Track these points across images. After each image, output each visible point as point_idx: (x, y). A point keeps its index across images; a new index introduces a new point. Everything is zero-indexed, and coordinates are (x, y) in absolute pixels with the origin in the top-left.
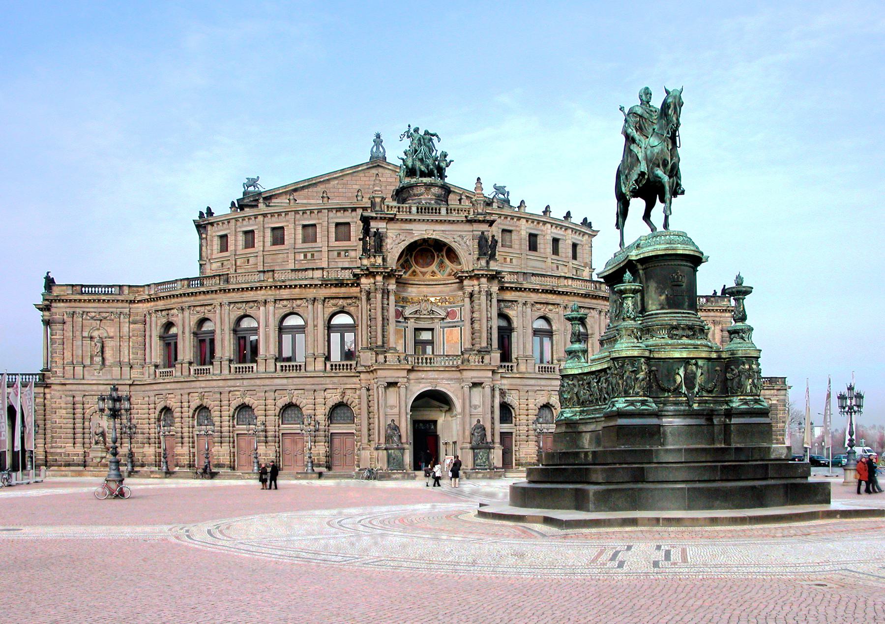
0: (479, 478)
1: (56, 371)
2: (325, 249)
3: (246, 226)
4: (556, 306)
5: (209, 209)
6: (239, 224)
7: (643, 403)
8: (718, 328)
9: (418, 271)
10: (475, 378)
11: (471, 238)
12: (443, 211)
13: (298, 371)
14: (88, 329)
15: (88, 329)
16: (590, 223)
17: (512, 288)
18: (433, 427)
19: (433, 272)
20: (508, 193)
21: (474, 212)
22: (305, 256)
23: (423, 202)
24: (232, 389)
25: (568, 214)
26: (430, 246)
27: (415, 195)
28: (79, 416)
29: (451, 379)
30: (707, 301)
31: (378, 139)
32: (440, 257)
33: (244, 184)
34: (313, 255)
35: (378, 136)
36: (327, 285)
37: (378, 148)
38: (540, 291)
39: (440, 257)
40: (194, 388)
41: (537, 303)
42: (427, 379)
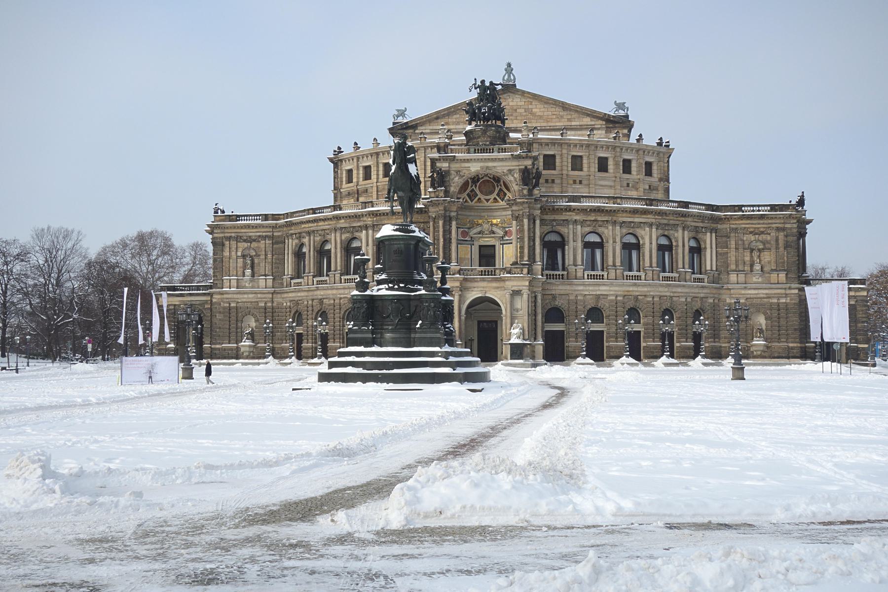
1: (217, 284)
3: (365, 162)
5: (339, 148)
6: (361, 160)
8: (782, 234)
9: (482, 199)
14: (240, 250)
15: (240, 250)
18: (494, 326)
19: (495, 199)
23: (481, 143)
24: (342, 296)
26: (490, 178)
27: (475, 138)
28: (233, 318)
29: (498, 288)
35: (509, 65)
37: (509, 76)
40: (316, 295)
41: (586, 220)
42: (478, 287)
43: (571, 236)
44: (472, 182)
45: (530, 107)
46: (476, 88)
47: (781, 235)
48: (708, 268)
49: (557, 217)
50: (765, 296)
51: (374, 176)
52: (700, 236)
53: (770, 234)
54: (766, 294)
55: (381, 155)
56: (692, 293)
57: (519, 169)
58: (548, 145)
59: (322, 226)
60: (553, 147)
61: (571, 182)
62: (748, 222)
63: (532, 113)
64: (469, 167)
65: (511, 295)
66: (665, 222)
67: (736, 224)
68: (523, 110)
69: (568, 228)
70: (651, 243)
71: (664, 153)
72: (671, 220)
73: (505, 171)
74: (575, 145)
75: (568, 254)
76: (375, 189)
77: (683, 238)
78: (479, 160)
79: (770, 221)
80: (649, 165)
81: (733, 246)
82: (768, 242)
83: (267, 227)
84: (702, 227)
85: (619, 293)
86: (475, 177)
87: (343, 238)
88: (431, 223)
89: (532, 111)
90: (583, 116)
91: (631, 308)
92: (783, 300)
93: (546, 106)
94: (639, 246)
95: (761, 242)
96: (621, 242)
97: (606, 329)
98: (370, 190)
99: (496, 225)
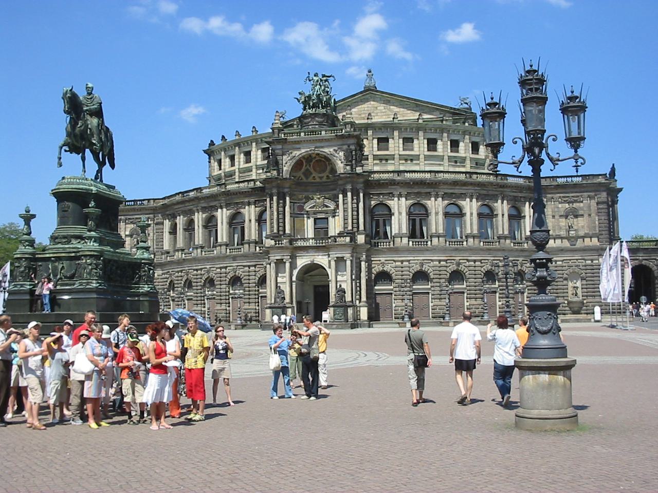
0: (333, 329)
5: (212, 141)
7: (22, 286)
26: (322, 158)
30: (583, 179)
36: (255, 191)
38: (412, 183)
39: (331, 166)
44: (306, 162)
47: (593, 203)
51: (236, 163)
52: (518, 204)
53: (582, 202)
58: (381, 129)
59: (188, 206)
60: (386, 131)
62: (564, 191)
66: (485, 192)
68: (383, 108)
72: (490, 190)
75: (395, 224)
76: (237, 174)
79: (583, 190)
81: (550, 213)
82: (582, 209)
83: (148, 210)
84: (521, 197)
86: (308, 158)
87: (204, 216)
88: (268, 199)
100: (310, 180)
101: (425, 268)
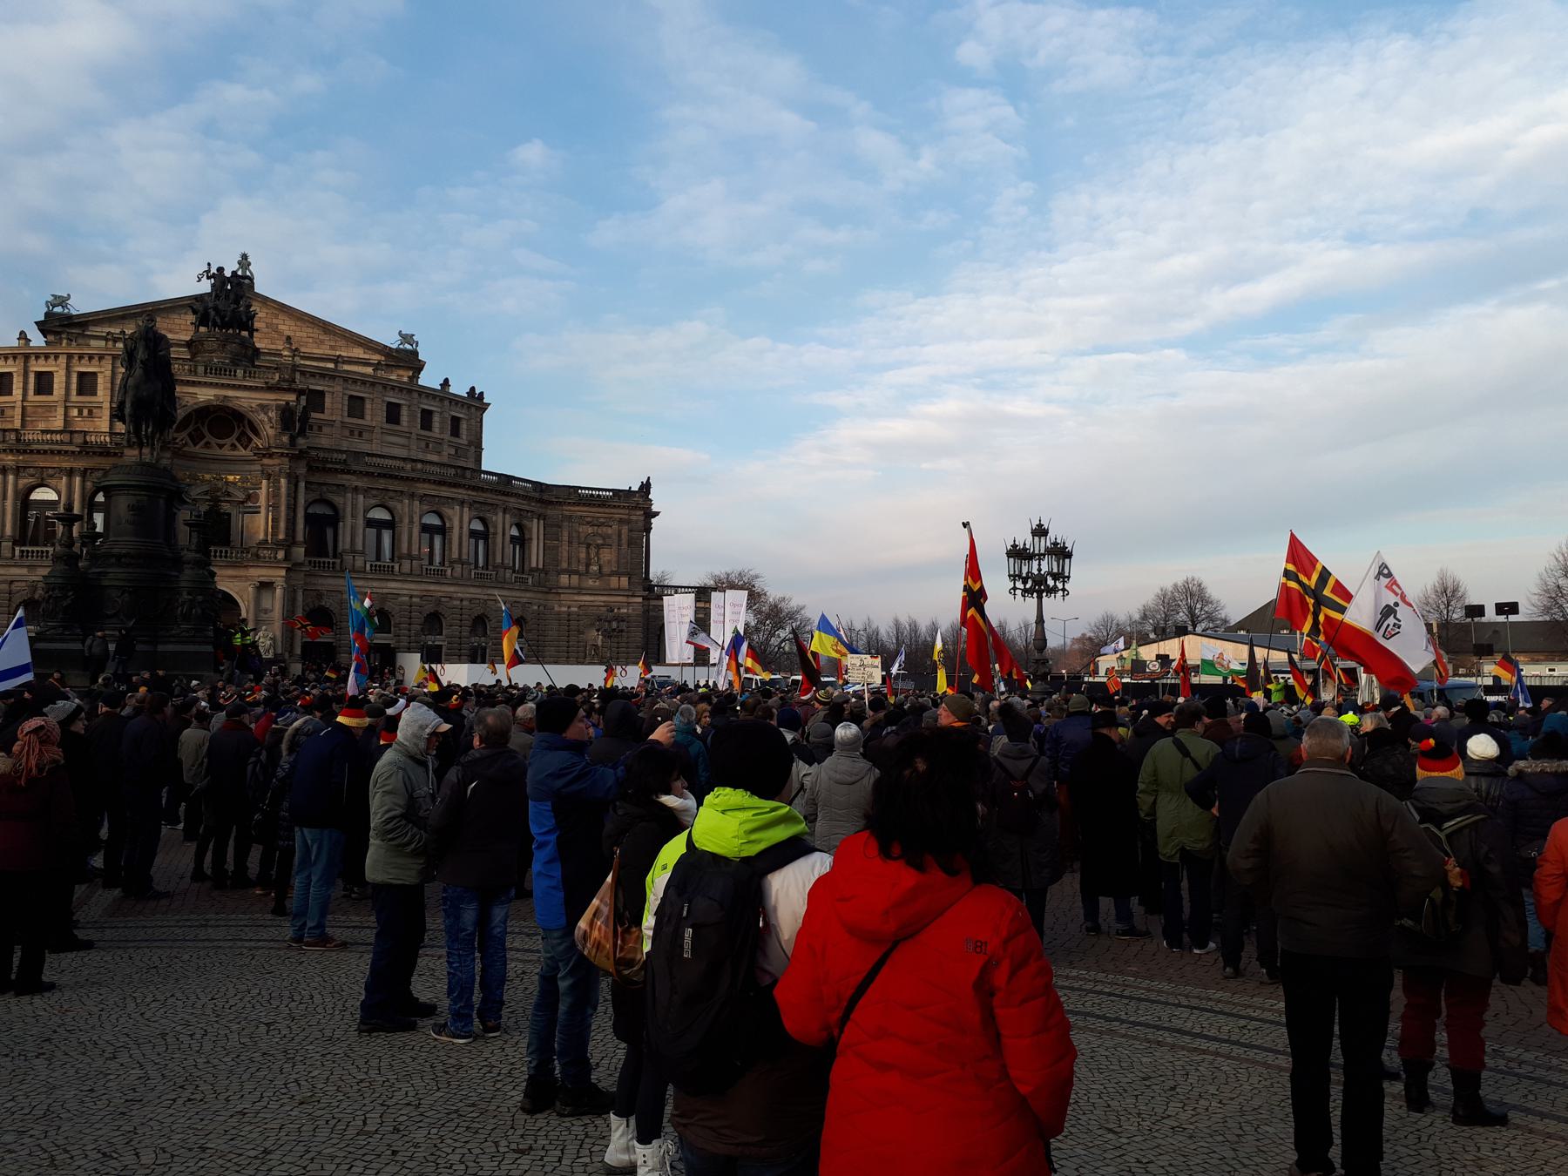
2: (107, 405)
4: (399, 494)
10: (263, 576)
11: (274, 408)
12: (240, 373)
13: (44, 558)
16: (481, 394)
17: (336, 469)
20: (417, 343)
21: (280, 377)
22: (80, 412)
23: (215, 360)
25: (446, 381)
31: (244, 261)
32: (242, 428)
33: (47, 302)
34: (90, 412)
35: (245, 257)
39: (242, 428)
43: (349, 509)
45: (275, 321)
46: (208, 278)
47: (625, 530)
48: (534, 565)
49: (330, 479)
50: (602, 604)
52: (525, 522)
54: (604, 602)
55: (33, 358)
56: (512, 597)
57: (278, 407)
61: (347, 433)
62: (585, 509)
63: (277, 331)
64: (196, 394)
65: (257, 587)
66: (481, 500)
67: (570, 511)
69: (344, 497)
70: (461, 528)
71: (477, 408)
73: (253, 405)
74: (355, 381)
76: (18, 411)
77: (504, 523)
78: (211, 385)
79: (613, 511)
80: (456, 421)
81: (566, 538)
82: (609, 537)
84: (528, 511)
85: (415, 593)
89: (277, 328)
90: (352, 345)
91: (431, 613)
92: (622, 611)
93: (298, 323)
94: (445, 530)
95: (600, 535)
96: (421, 524)
97: (394, 641)
98: (8, 412)
99: (234, 483)
100: (198, 449)
101: (388, 606)
